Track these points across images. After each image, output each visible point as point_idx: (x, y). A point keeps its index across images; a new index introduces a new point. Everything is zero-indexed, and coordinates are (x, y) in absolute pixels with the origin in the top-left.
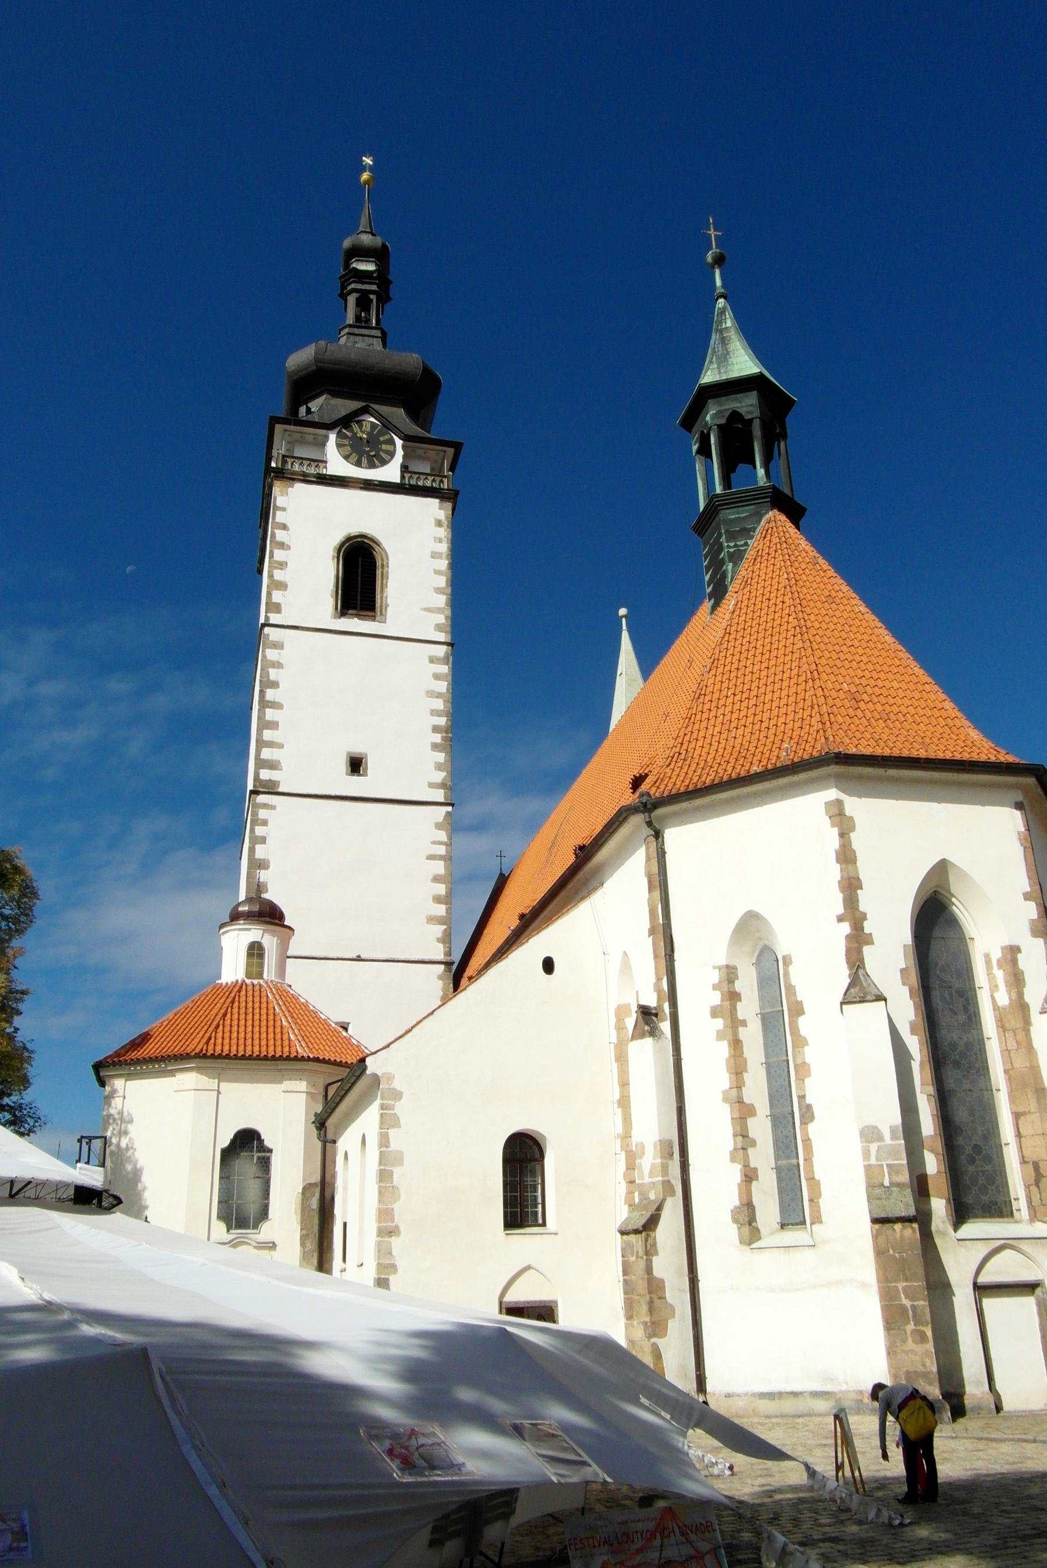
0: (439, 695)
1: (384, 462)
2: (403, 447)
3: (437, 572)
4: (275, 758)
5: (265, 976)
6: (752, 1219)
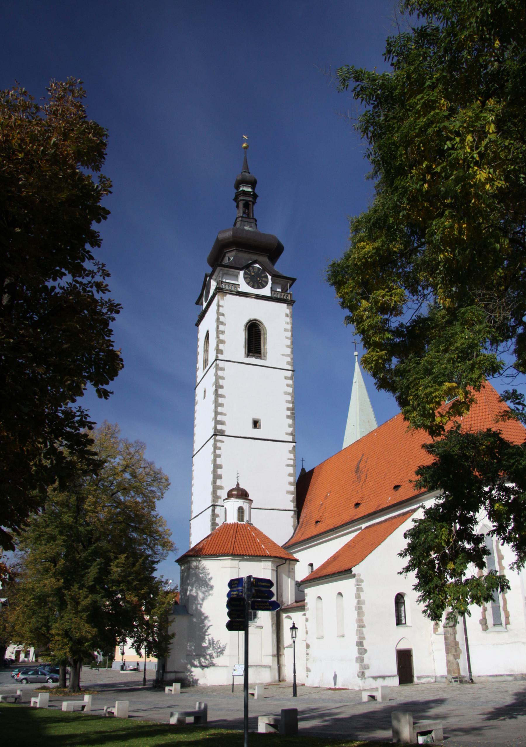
0: (289, 394)
1: (264, 286)
2: (272, 279)
3: (287, 338)
4: (223, 420)
5: (245, 520)
6: (486, 623)
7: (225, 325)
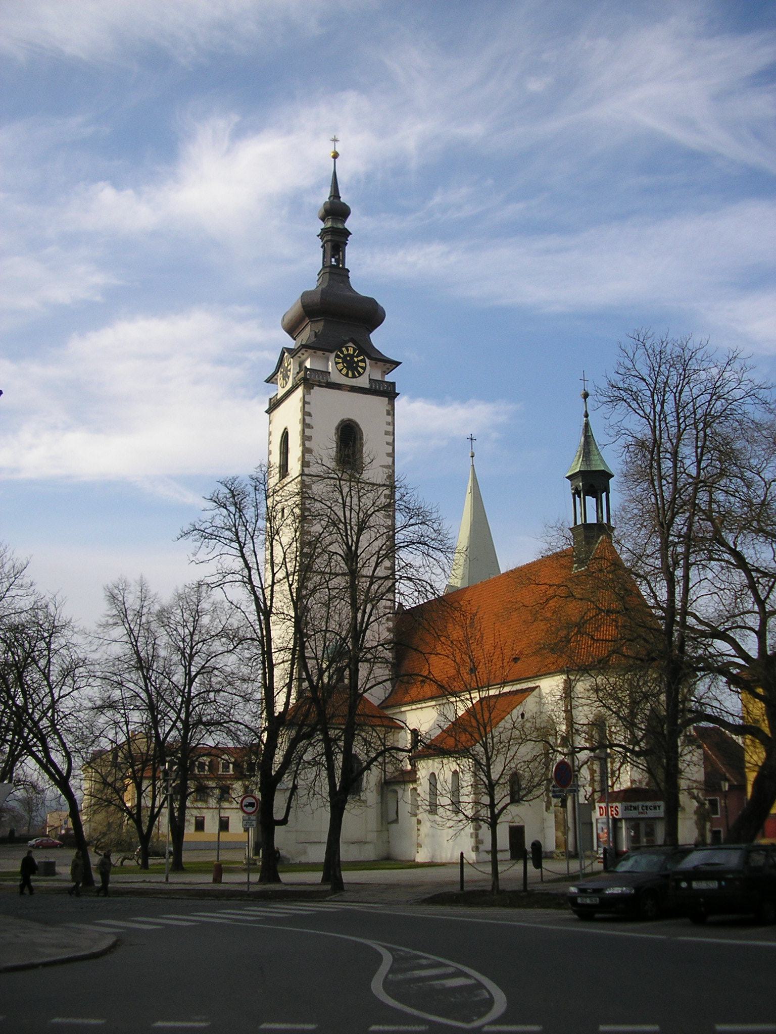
1: (360, 374)
7: (313, 428)
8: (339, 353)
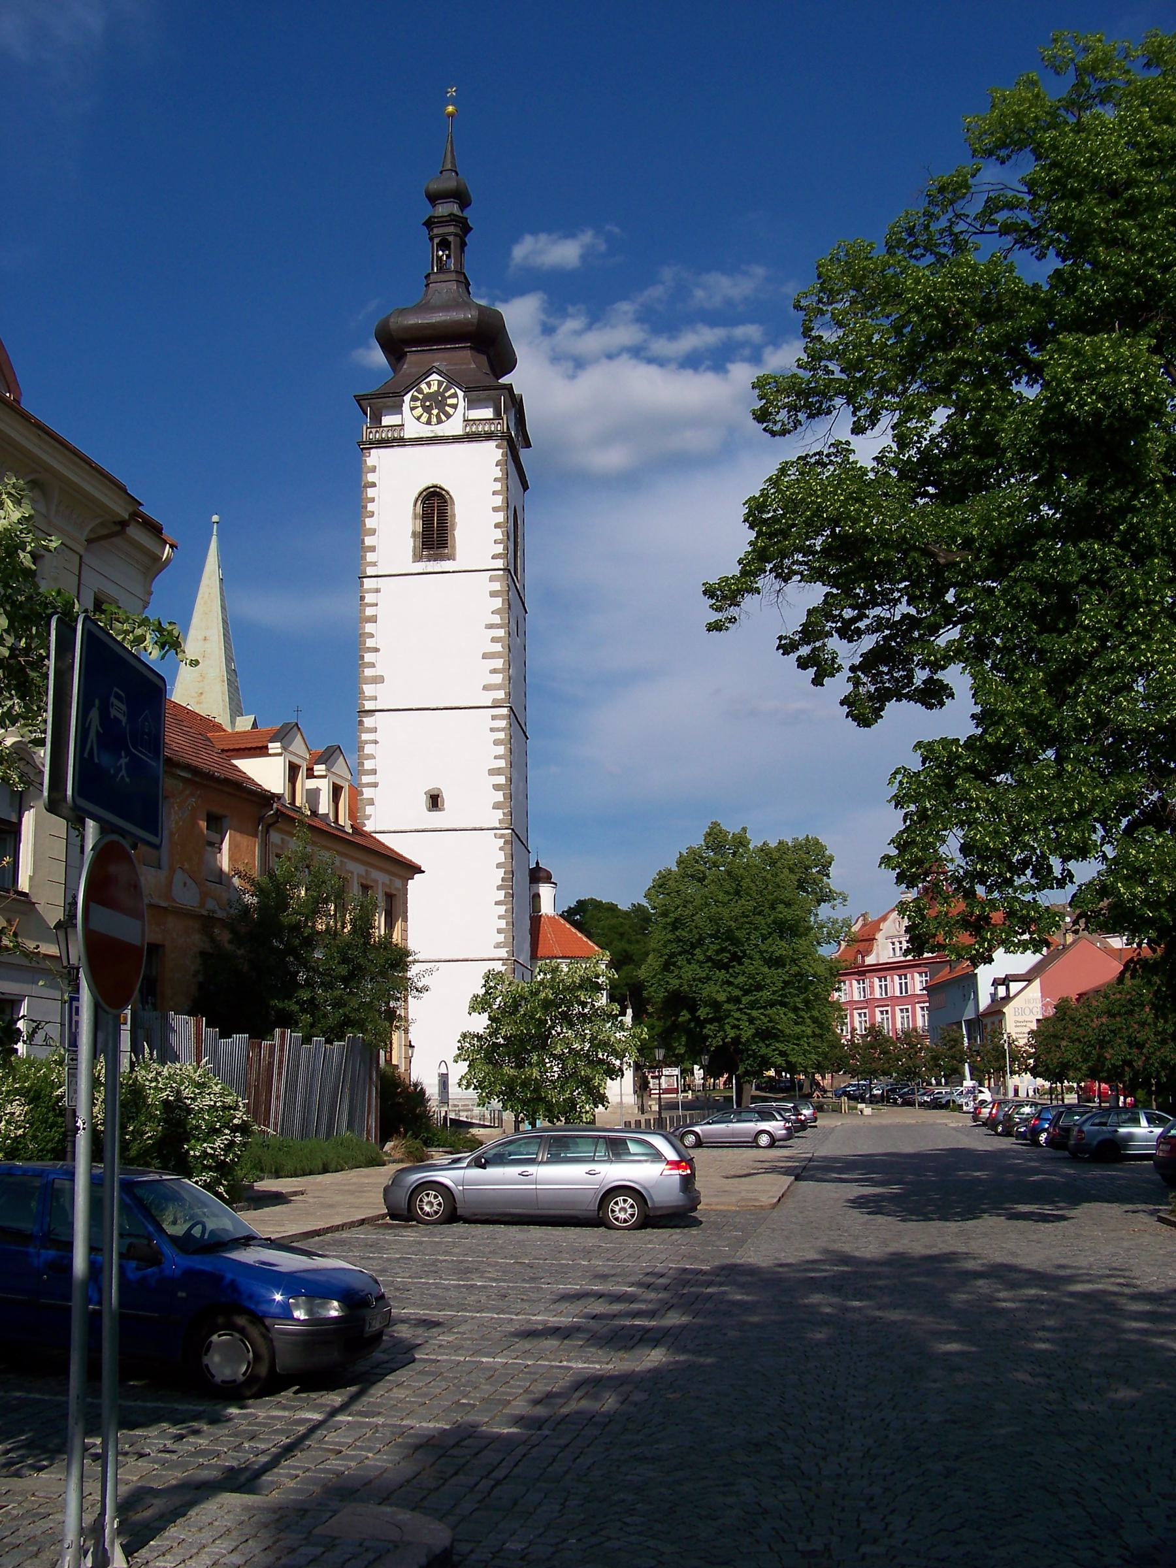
1: (448, 416)
8: (416, 394)
